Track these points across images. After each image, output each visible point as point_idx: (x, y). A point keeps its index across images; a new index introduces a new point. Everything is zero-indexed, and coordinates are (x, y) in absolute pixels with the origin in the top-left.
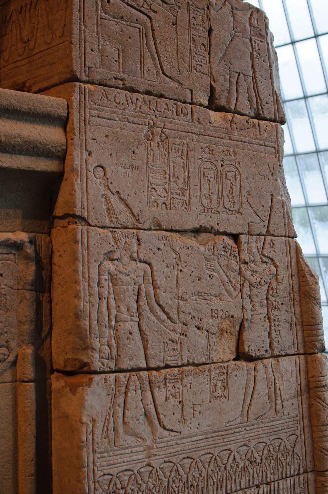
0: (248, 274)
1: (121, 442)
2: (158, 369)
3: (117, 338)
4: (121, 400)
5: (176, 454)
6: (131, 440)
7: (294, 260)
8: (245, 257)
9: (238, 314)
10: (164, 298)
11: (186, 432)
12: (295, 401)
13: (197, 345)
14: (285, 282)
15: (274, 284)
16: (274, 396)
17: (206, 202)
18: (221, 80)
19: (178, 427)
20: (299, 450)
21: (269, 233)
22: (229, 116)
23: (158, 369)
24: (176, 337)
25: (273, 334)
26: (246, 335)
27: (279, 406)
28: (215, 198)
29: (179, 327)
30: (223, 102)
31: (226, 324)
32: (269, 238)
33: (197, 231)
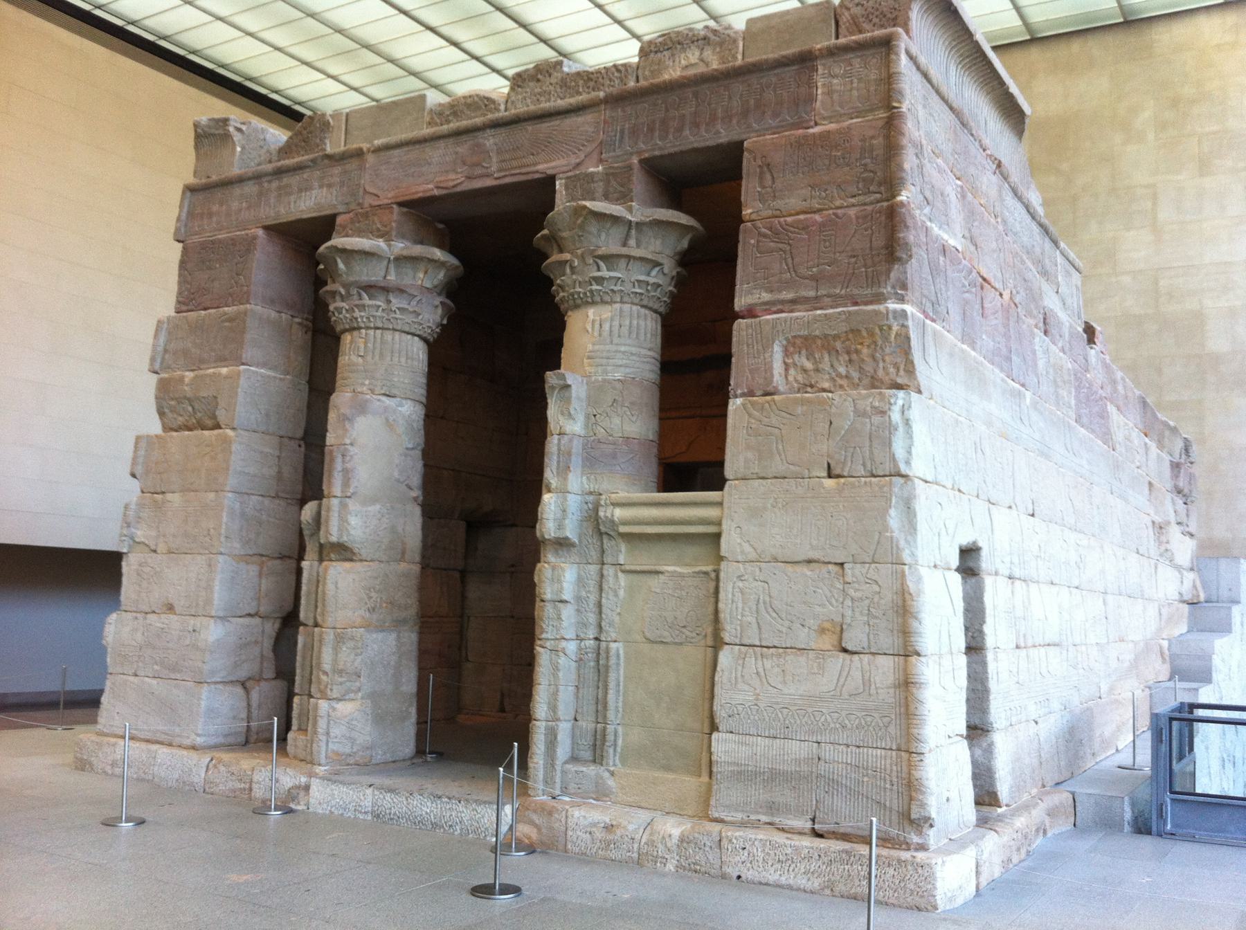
0: (851, 592)
1: (739, 686)
2: (768, 647)
3: (741, 626)
4: (741, 662)
5: (777, 703)
6: (746, 687)
7: (899, 582)
8: (849, 579)
9: (838, 619)
10: (776, 603)
11: (786, 691)
12: (892, 691)
13: (802, 637)
14: (888, 597)
15: (876, 600)
16: (867, 683)
17: (814, 543)
18: (837, 456)
19: (780, 686)
20: (892, 729)
21: (874, 562)
22: (842, 480)
23: (768, 647)
24: (784, 630)
25: (871, 636)
26: (845, 635)
27: (873, 691)
28: (822, 539)
29: (787, 623)
30: (837, 471)
31: (827, 625)
32: (873, 566)
33: (809, 562)
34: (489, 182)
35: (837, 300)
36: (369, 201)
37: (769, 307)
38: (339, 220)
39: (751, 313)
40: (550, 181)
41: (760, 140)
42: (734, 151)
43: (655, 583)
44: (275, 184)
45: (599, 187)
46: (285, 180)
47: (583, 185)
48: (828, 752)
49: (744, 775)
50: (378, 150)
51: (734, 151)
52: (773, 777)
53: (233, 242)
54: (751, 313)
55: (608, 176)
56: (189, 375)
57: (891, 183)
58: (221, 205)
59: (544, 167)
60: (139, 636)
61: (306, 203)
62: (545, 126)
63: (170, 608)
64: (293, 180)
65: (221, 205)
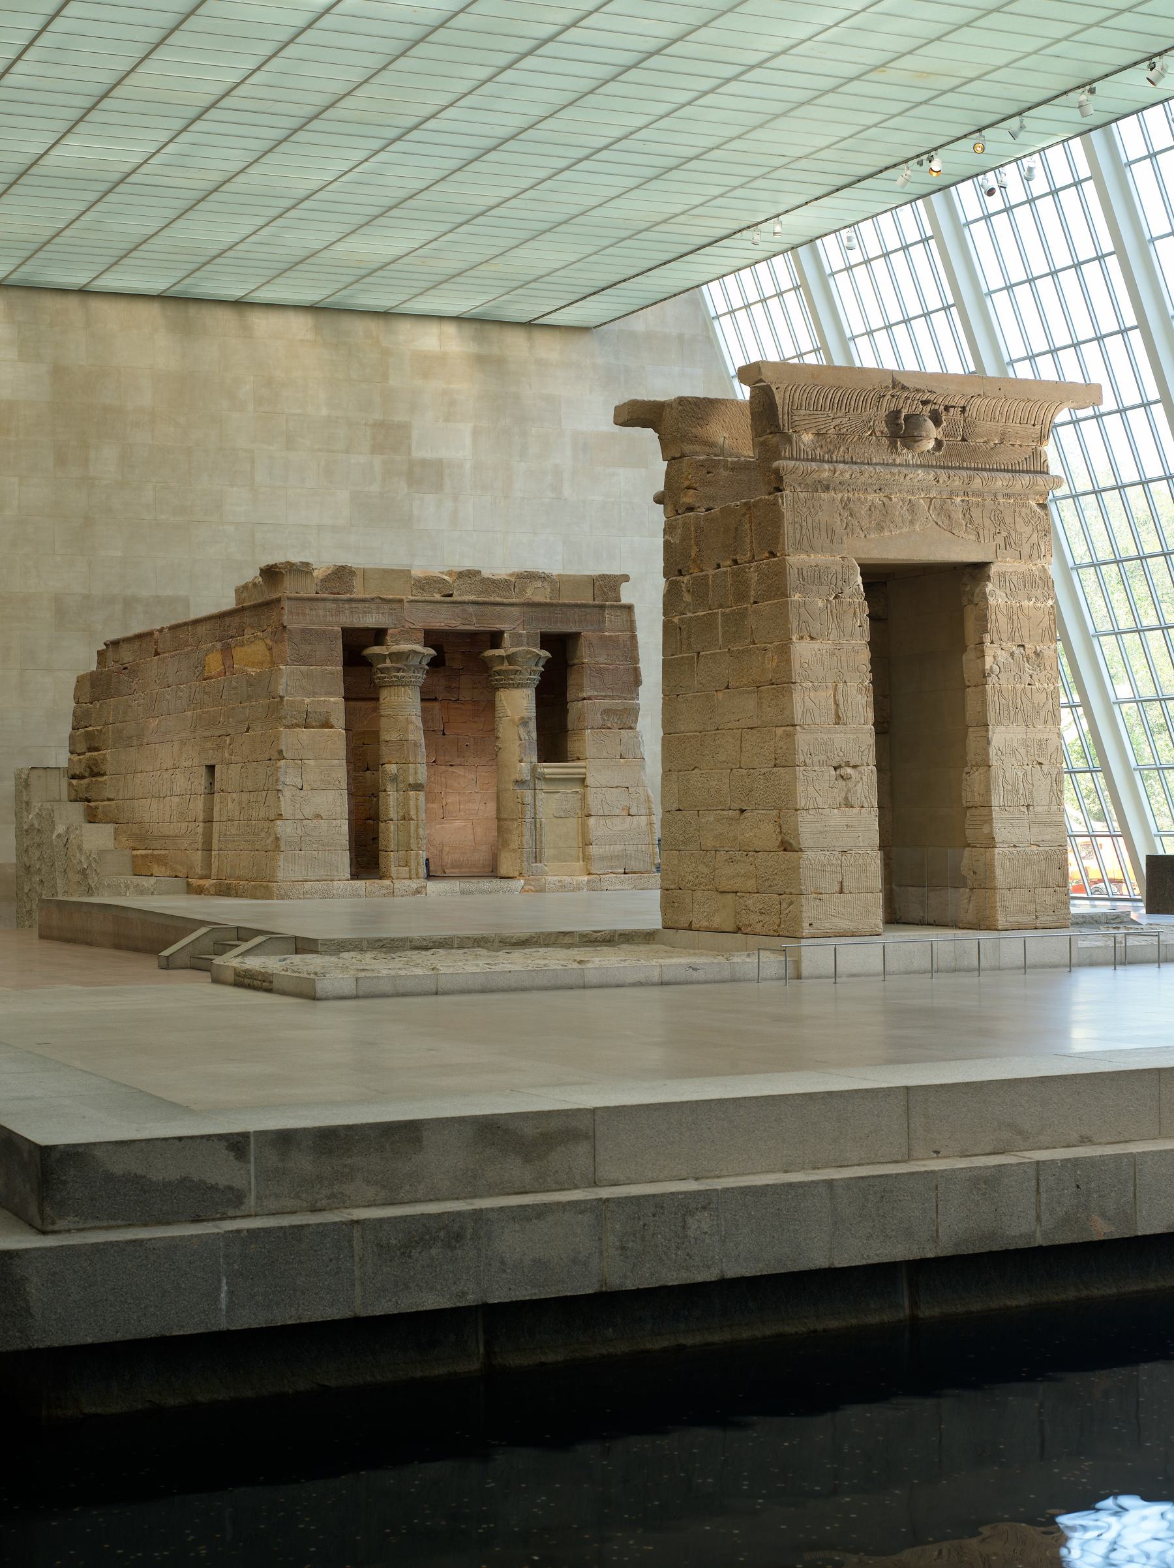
13: (617, 812)
34: (472, 628)
35: (620, 698)
36: (407, 625)
37: (596, 697)
38: (390, 631)
39: (589, 698)
40: (502, 633)
41: (588, 633)
42: (576, 636)
43: (556, 796)
44: (347, 606)
45: (525, 640)
46: (354, 605)
47: (517, 639)
48: (628, 847)
49: (602, 858)
50: (412, 601)
51: (576, 636)
52: (611, 858)
53: (324, 632)
54: (589, 698)
55: (529, 636)
56: (307, 700)
57: (636, 660)
58: (311, 610)
59: (499, 626)
60: (299, 832)
61: (371, 620)
62: (497, 608)
63: (318, 816)
64: (360, 606)
65: (311, 610)
